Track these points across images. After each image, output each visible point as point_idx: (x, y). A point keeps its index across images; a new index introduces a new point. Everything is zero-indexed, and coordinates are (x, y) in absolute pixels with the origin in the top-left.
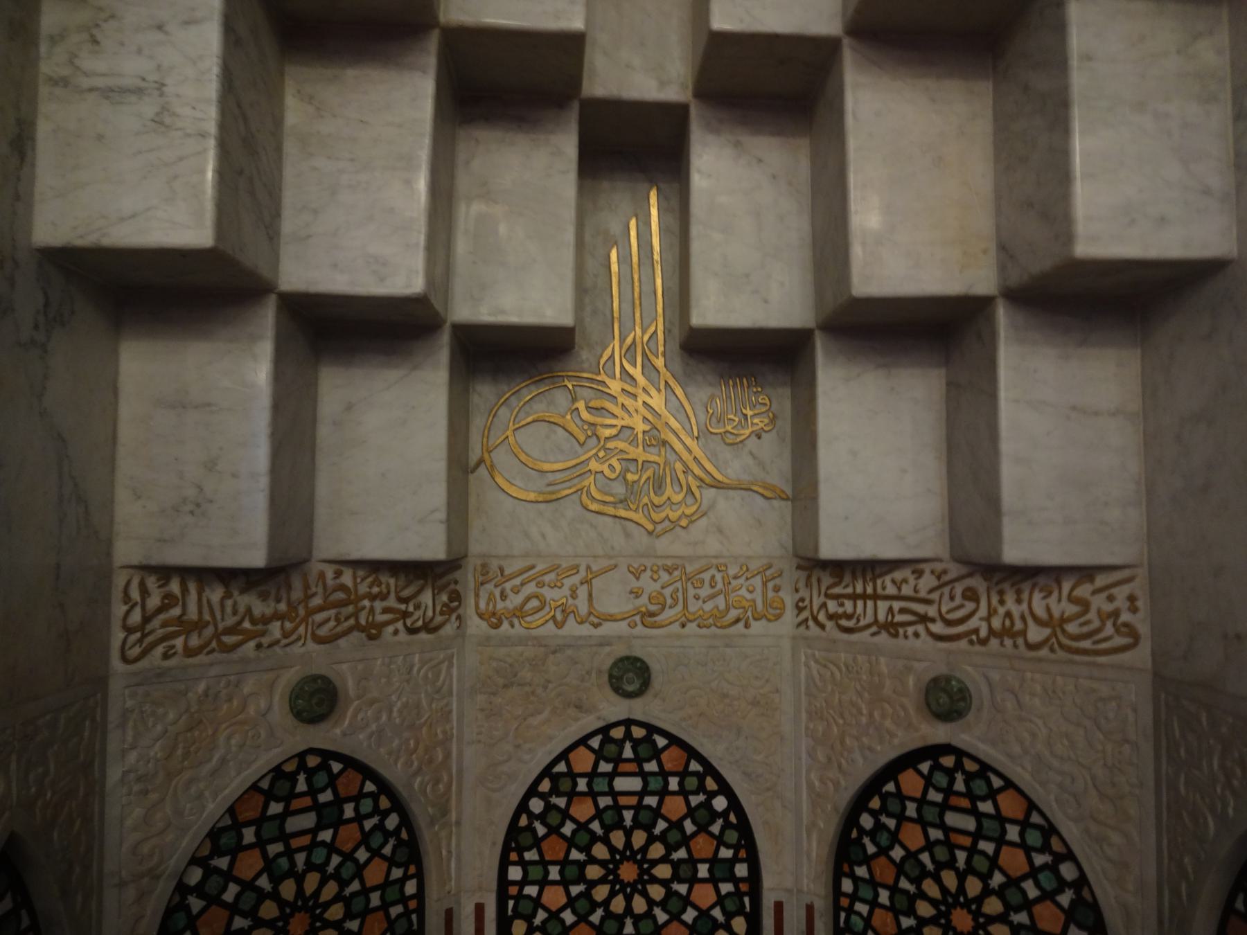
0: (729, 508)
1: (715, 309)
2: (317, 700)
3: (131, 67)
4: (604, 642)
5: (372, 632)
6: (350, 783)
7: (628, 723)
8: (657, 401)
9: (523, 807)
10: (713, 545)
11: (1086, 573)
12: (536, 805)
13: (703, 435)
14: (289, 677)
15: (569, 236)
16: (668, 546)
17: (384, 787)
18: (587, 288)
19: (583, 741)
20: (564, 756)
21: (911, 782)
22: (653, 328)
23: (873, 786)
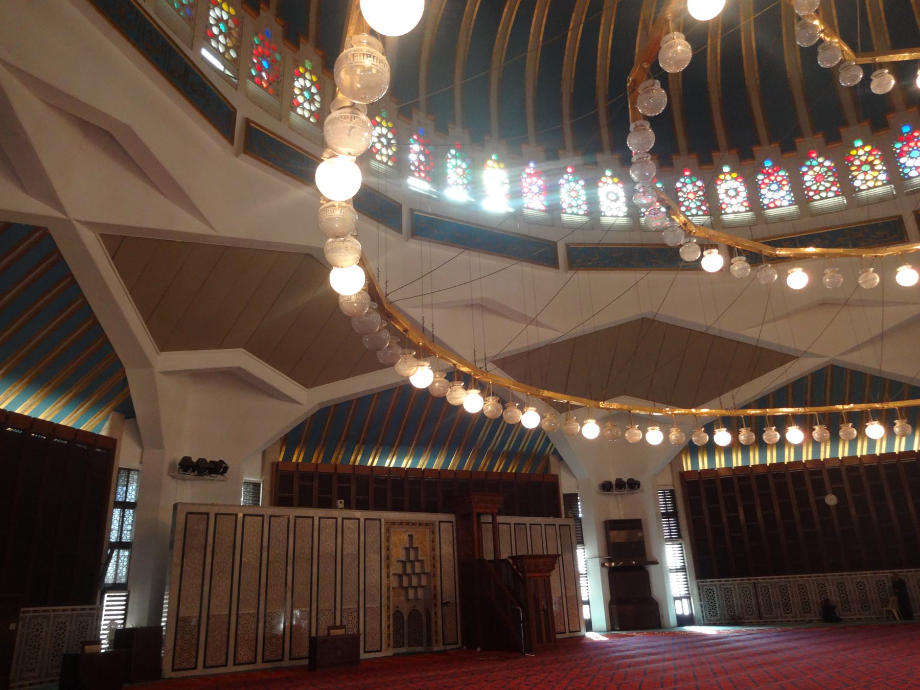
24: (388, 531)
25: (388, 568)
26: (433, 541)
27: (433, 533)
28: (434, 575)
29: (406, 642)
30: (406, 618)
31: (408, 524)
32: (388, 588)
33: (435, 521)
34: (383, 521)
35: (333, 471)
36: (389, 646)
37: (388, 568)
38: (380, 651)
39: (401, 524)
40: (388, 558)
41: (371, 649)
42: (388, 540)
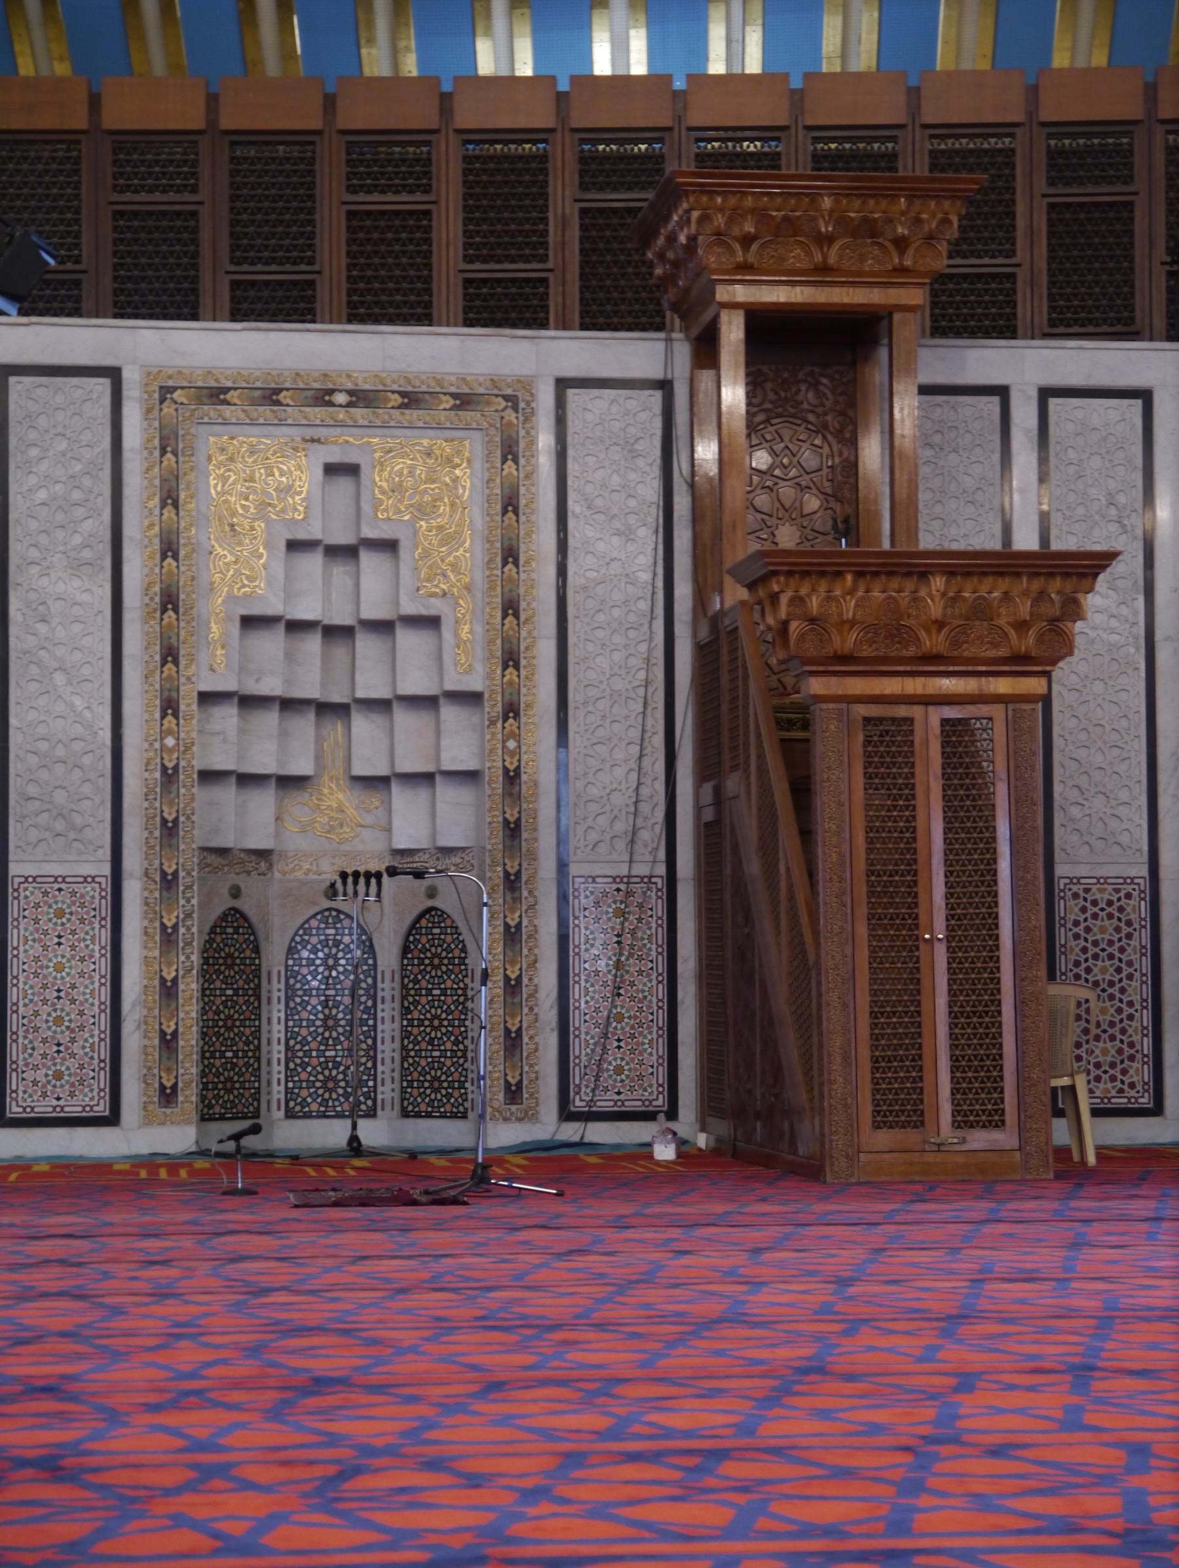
0: (366, 834)
1: (359, 770)
2: (236, 893)
3: (217, 727)
4: (323, 881)
5: (248, 873)
6: (241, 921)
7: (329, 909)
8: (340, 796)
9: (293, 939)
10: (361, 847)
11: (463, 849)
12: (298, 939)
13: (357, 808)
14: (229, 884)
15: (312, 740)
16: (345, 847)
17: (250, 926)
18: (319, 758)
19: (314, 916)
20: (307, 921)
21: (424, 922)
22: (339, 769)
23: (413, 926)
24: (167, 442)
25: (170, 654)
26: (511, 504)
27: (510, 451)
28: (512, 710)
29: (387, 1092)
30: (388, 957)
31: (323, 398)
32: (169, 776)
33: (527, 384)
34: (130, 376)
35: (79, 120)
36: (168, 1096)
37: (170, 654)
38: (112, 1119)
39: (271, 396)
40: (169, 601)
41: (44, 1108)
42: (170, 498)
